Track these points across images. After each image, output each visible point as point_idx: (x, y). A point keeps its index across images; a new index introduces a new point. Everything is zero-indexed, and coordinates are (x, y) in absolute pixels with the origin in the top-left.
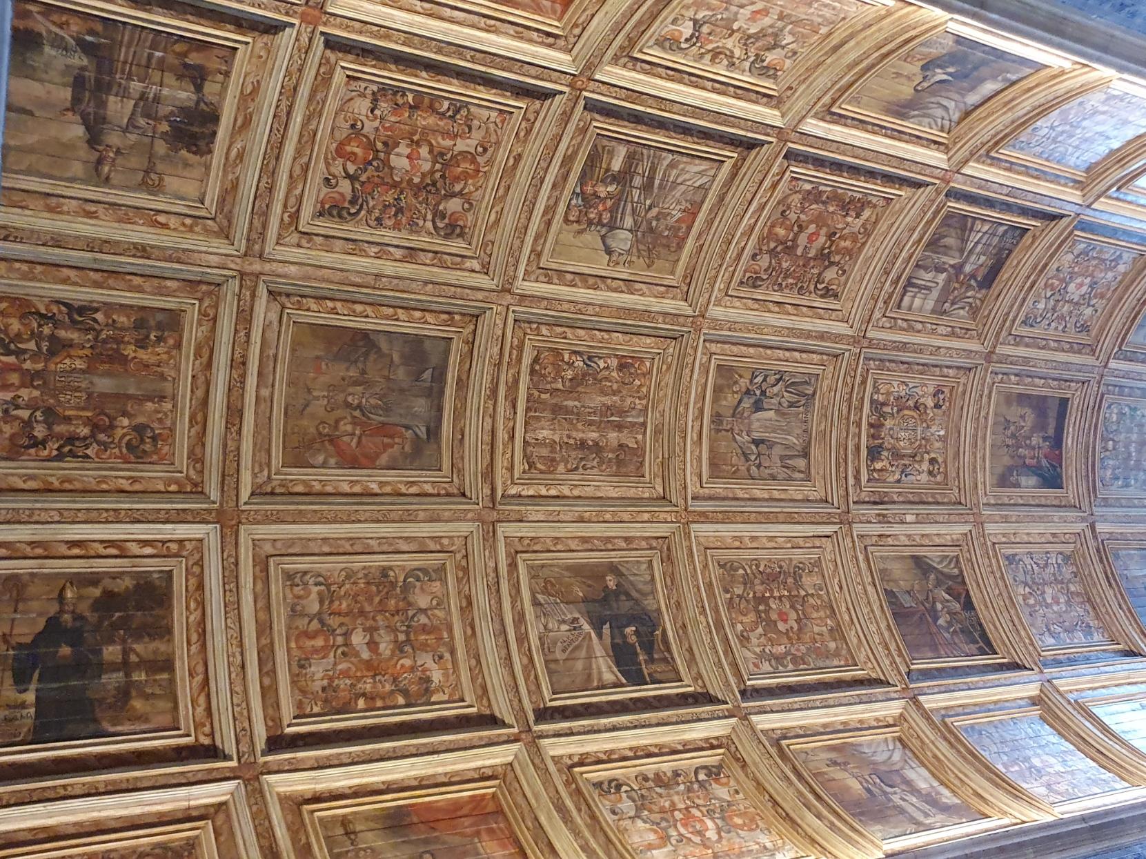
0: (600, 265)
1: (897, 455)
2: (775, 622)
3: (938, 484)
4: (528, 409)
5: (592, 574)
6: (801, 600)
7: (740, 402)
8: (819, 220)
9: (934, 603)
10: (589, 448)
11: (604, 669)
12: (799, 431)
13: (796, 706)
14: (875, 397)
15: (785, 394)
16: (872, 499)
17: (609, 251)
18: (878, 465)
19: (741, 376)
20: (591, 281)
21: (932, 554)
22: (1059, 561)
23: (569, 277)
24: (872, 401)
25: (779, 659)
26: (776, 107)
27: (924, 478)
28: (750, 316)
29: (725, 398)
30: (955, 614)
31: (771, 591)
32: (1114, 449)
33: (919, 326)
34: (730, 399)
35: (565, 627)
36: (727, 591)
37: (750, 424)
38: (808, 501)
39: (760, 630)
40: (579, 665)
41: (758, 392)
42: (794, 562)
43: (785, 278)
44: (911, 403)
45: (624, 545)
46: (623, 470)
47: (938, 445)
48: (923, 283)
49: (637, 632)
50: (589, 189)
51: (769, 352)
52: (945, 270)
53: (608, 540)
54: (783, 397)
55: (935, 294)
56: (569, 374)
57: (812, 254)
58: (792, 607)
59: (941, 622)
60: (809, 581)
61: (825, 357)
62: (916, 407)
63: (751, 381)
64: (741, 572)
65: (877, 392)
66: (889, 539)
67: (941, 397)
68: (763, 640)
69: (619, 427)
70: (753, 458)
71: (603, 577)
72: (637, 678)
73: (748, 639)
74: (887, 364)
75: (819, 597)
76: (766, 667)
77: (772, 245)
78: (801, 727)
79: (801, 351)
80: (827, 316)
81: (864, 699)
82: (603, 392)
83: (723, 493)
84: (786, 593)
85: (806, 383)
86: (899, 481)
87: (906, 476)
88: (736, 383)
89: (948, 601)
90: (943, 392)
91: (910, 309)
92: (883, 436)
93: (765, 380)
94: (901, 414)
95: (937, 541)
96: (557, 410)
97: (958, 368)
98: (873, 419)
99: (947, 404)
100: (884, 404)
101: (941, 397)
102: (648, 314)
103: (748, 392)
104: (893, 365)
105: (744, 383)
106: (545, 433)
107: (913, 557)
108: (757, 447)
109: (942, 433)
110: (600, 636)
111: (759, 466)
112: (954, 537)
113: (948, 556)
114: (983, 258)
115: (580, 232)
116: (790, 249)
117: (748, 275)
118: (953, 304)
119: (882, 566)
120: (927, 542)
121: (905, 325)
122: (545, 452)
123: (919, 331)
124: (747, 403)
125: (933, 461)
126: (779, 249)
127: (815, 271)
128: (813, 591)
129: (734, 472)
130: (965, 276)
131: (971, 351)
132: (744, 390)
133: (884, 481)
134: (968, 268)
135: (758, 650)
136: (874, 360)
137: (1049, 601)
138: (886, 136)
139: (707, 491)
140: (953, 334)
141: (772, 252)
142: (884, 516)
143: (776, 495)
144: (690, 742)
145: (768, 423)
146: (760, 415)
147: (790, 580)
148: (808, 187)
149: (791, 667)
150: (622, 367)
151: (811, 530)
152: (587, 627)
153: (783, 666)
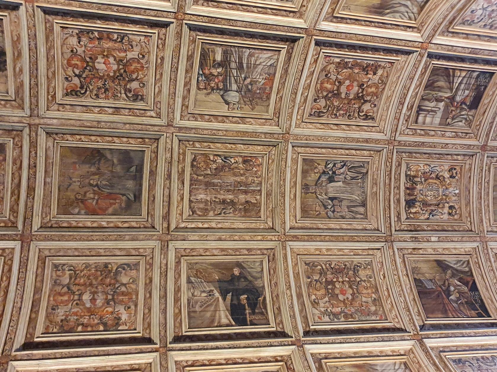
0: (224, 110)
1: (425, 204)
2: (337, 295)
3: (456, 220)
4: (191, 185)
5: (226, 267)
6: (356, 284)
7: (320, 178)
8: (350, 77)
9: (449, 286)
10: (228, 203)
11: (223, 316)
12: (359, 193)
13: (338, 341)
14: (409, 173)
15: (348, 173)
16: (409, 229)
17: (227, 103)
18: (413, 210)
19: (319, 164)
20: (220, 119)
21: (451, 260)
23: (207, 117)
24: (407, 175)
25: (336, 315)
26: (300, 17)
27: (446, 217)
28: (319, 132)
29: (310, 176)
30: (463, 293)
31: (338, 278)
33: (433, 133)
34: (313, 177)
35: (204, 295)
36: (309, 278)
37: (326, 190)
38: (366, 230)
39: (327, 299)
40: (208, 314)
41: (330, 173)
42: (355, 263)
43: (338, 110)
44: (433, 175)
45: (247, 253)
46: (248, 214)
47: (454, 198)
48: (430, 108)
49: (248, 299)
50: (207, 72)
51: (335, 151)
52: (442, 101)
53: (237, 250)
54: (347, 174)
55: (439, 114)
56: (214, 166)
57: (352, 96)
58: (351, 287)
59: (452, 297)
60: (362, 274)
61: (372, 152)
62: (437, 178)
63: (326, 167)
64: (319, 267)
65: (410, 170)
66: (420, 251)
67: (454, 172)
68: (327, 304)
69: (246, 192)
70: (329, 207)
71: (232, 269)
72: (241, 321)
73: (318, 304)
74: (414, 155)
75: (369, 282)
76: (327, 319)
77: (325, 94)
78: (339, 353)
79: (356, 150)
80: (369, 130)
81: (386, 339)
82: (235, 175)
83: (310, 226)
84: (347, 279)
85: (361, 166)
86: (428, 219)
87: (433, 216)
88: (316, 168)
89: (459, 286)
90: (455, 169)
91: (424, 123)
92: (416, 193)
93: (334, 165)
94: (427, 182)
95: (454, 252)
96: (208, 184)
97: (464, 155)
98: (408, 185)
99: (459, 176)
100: (415, 177)
101: (454, 172)
102: (255, 134)
103: (324, 172)
104: (419, 155)
105: (321, 168)
106: (201, 196)
107: (436, 261)
108: (332, 201)
109: (457, 192)
110: (224, 299)
111: (333, 212)
112: (467, 250)
113: (462, 260)
114: (467, 92)
115: (208, 94)
116: (337, 95)
117: (314, 111)
118: (453, 119)
119: (414, 265)
120: (447, 252)
121: (422, 132)
122: (202, 206)
123: (433, 136)
124: (324, 178)
125: (451, 207)
126: (330, 95)
127: (356, 106)
128: (366, 279)
129: (318, 215)
130: (458, 103)
131: (470, 145)
132: (321, 171)
133: (418, 219)
134: (458, 99)
135: (323, 310)
136: (405, 152)
138: (376, 27)
139: (300, 225)
140: (457, 136)
141: (325, 97)
142: (416, 238)
143: (345, 226)
144: (263, 358)
145: (338, 189)
146: (332, 184)
147: (351, 272)
148: (338, 60)
149: (343, 319)
150: (245, 162)
151: (366, 245)
152: (217, 294)
153: (339, 319)
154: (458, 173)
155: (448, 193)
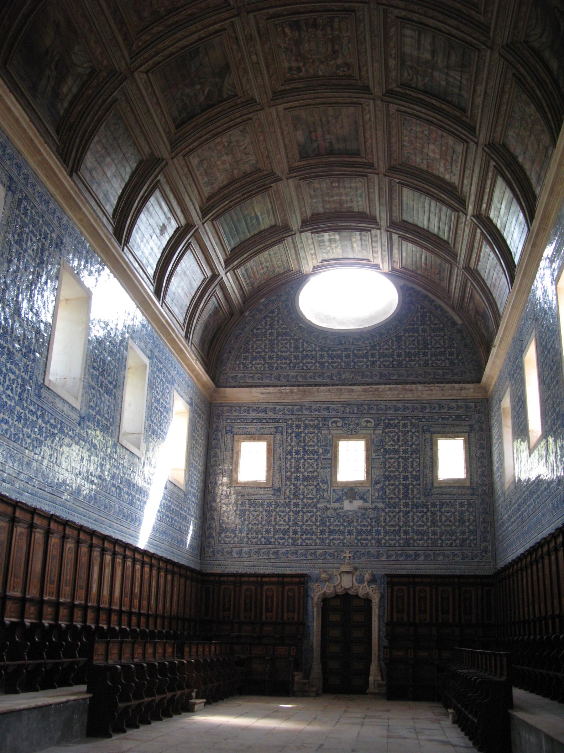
18: (287, 30)
22: (251, 162)
27: (286, 65)
32: (333, 187)
44: (337, 47)
62: (335, 52)
67: (345, 69)
87: (284, 51)
90: (349, 69)
99: (341, 74)
125: (299, 69)
137: (223, 158)
154: (345, 73)
155: (317, 64)
